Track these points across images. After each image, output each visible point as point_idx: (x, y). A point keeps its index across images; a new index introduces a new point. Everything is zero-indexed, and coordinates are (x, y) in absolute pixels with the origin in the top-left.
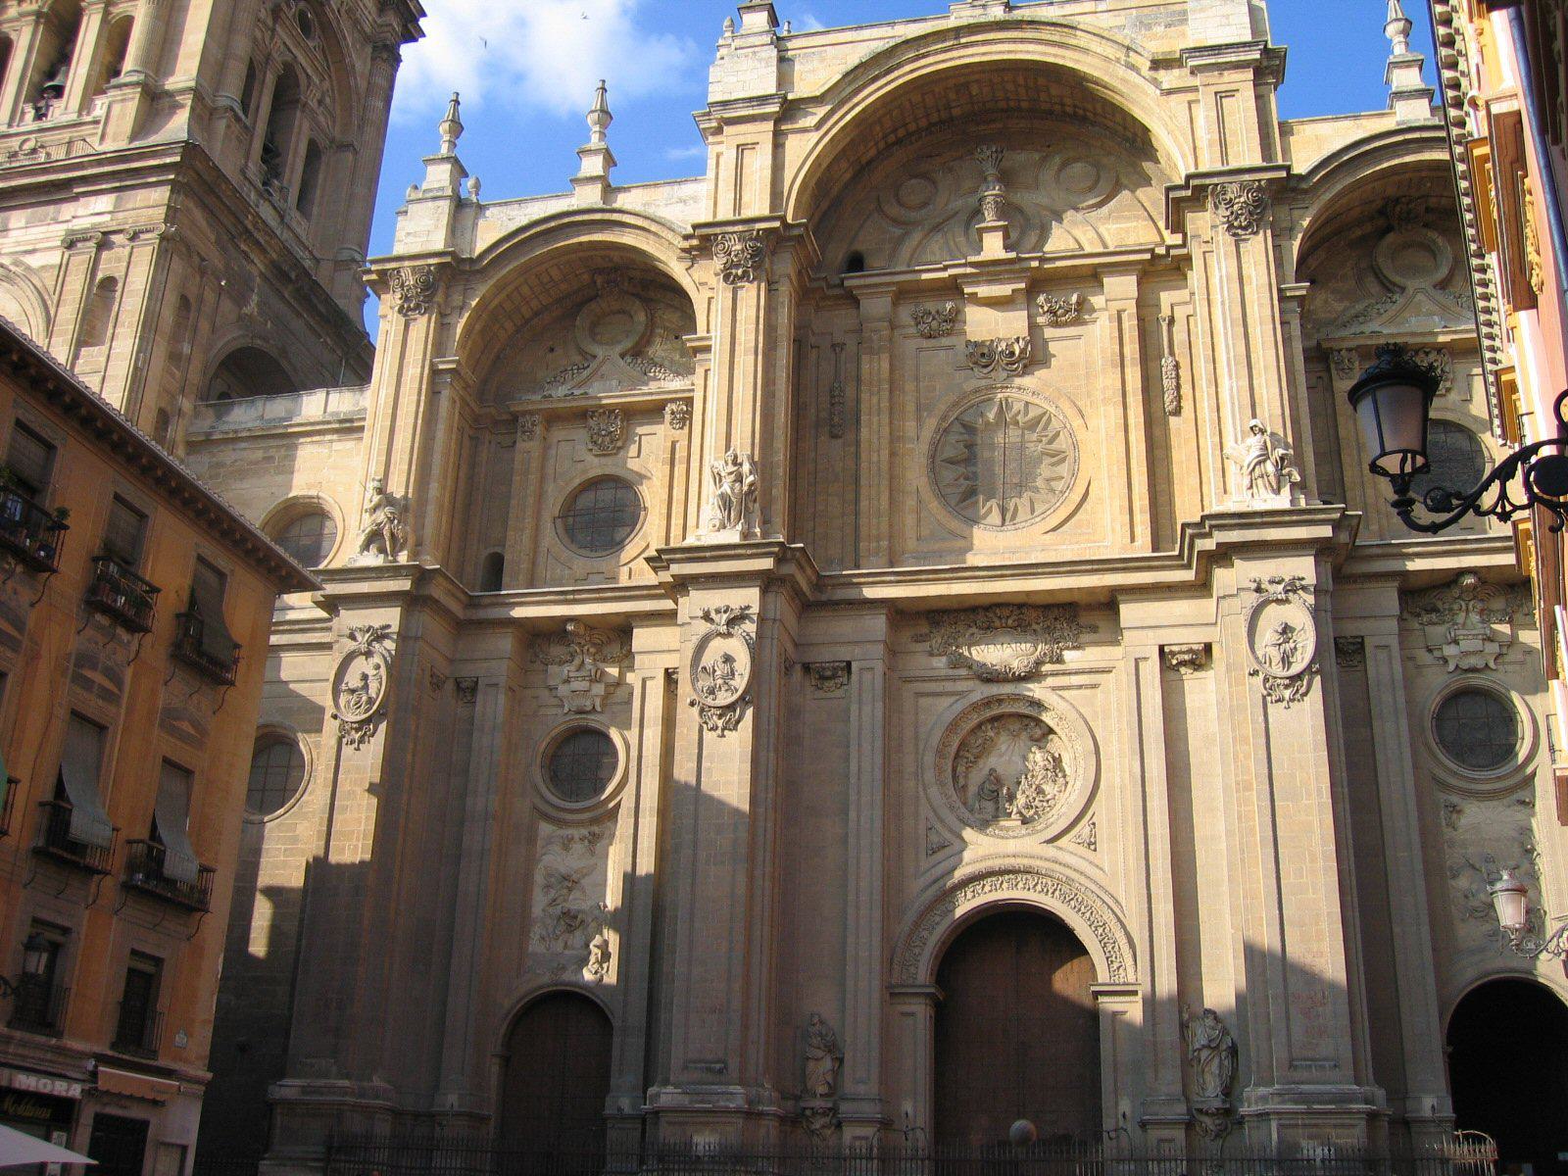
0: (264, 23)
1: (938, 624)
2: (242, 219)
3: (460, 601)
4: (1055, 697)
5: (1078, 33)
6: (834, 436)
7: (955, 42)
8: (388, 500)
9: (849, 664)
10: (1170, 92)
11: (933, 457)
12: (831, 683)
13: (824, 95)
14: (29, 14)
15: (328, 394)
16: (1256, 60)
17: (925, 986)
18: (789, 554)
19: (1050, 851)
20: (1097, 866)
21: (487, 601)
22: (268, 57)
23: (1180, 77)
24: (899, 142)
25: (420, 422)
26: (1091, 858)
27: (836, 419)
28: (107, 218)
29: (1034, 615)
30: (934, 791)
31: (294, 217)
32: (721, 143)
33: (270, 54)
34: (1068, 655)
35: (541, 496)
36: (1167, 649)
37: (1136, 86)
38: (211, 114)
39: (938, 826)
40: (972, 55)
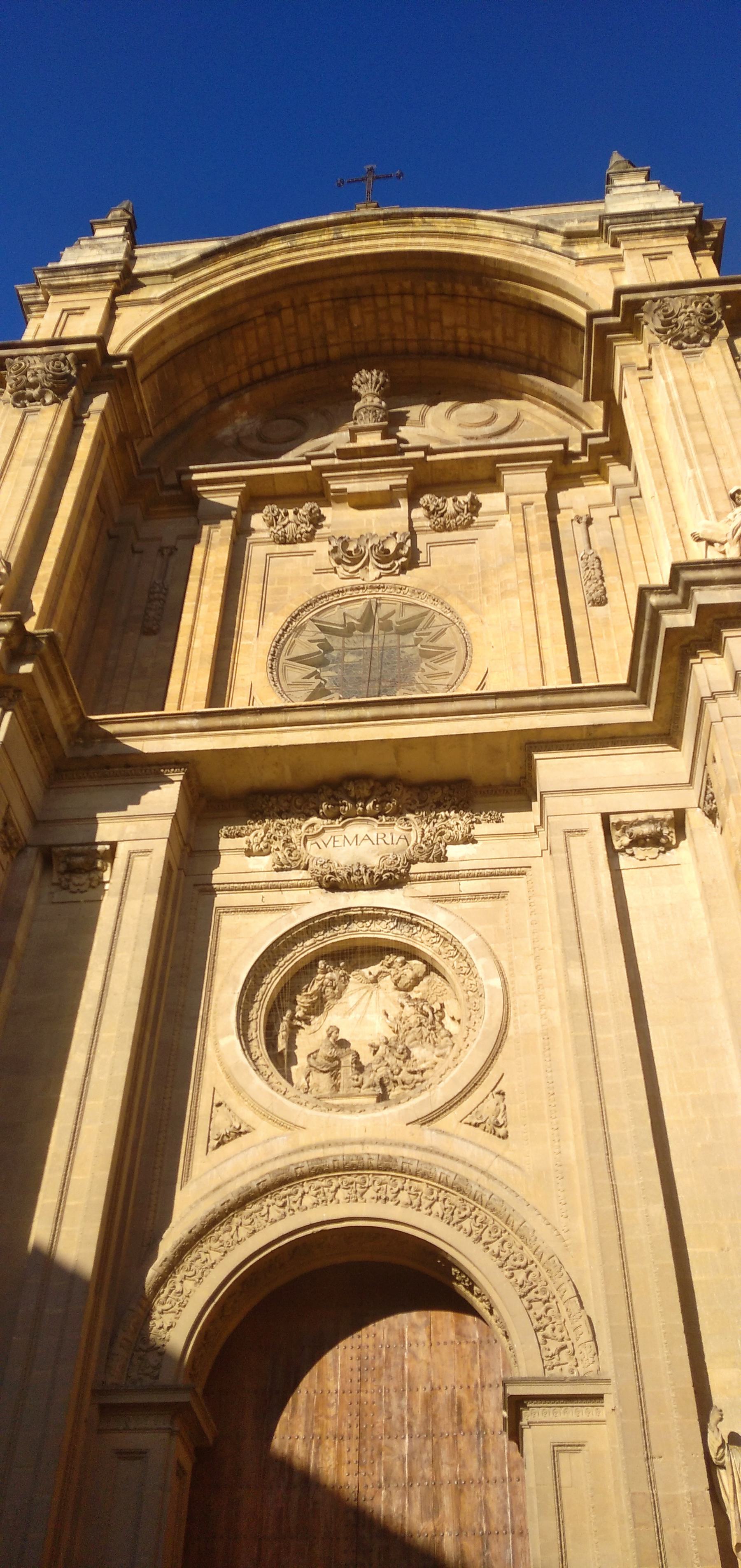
1: (262, 813)
4: (438, 909)
5: (479, 222)
6: (148, 632)
7: (335, 237)
9: (114, 845)
10: (588, 262)
11: (274, 656)
12: (83, 879)
13: (175, 272)
16: (689, 227)
17: (176, 1389)
18: (29, 648)
19: (428, 1136)
20: (511, 1163)
23: (599, 249)
24: (266, 379)
26: (499, 1151)
27: (152, 614)
29: (406, 796)
30: (230, 1041)
34: (453, 851)
36: (613, 819)
37: (546, 263)
39: (233, 1100)
40: (355, 249)
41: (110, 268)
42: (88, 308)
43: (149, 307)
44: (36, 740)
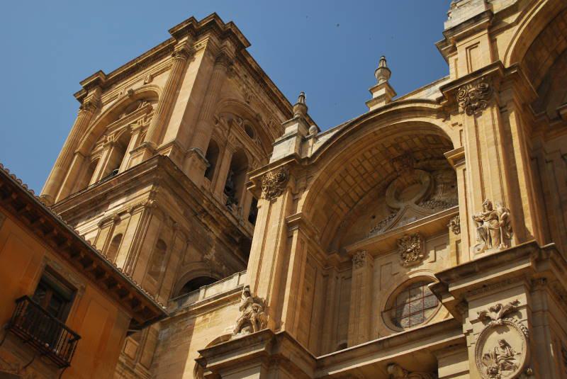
0: (224, 127)
2: (199, 202)
3: (306, 361)
8: (257, 300)
14: (108, 145)
15: (240, 275)
18: (544, 256)
21: (328, 362)
22: (226, 142)
25: (278, 252)
28: (122, 206)
31: (247, 224)
32: (457, 54)
33: (227, 141)
35: (371, 301)
38: (185, 157)
41: (483, 16)
42: (479, 42)
43: (511, 29)
44: (559, 300)
